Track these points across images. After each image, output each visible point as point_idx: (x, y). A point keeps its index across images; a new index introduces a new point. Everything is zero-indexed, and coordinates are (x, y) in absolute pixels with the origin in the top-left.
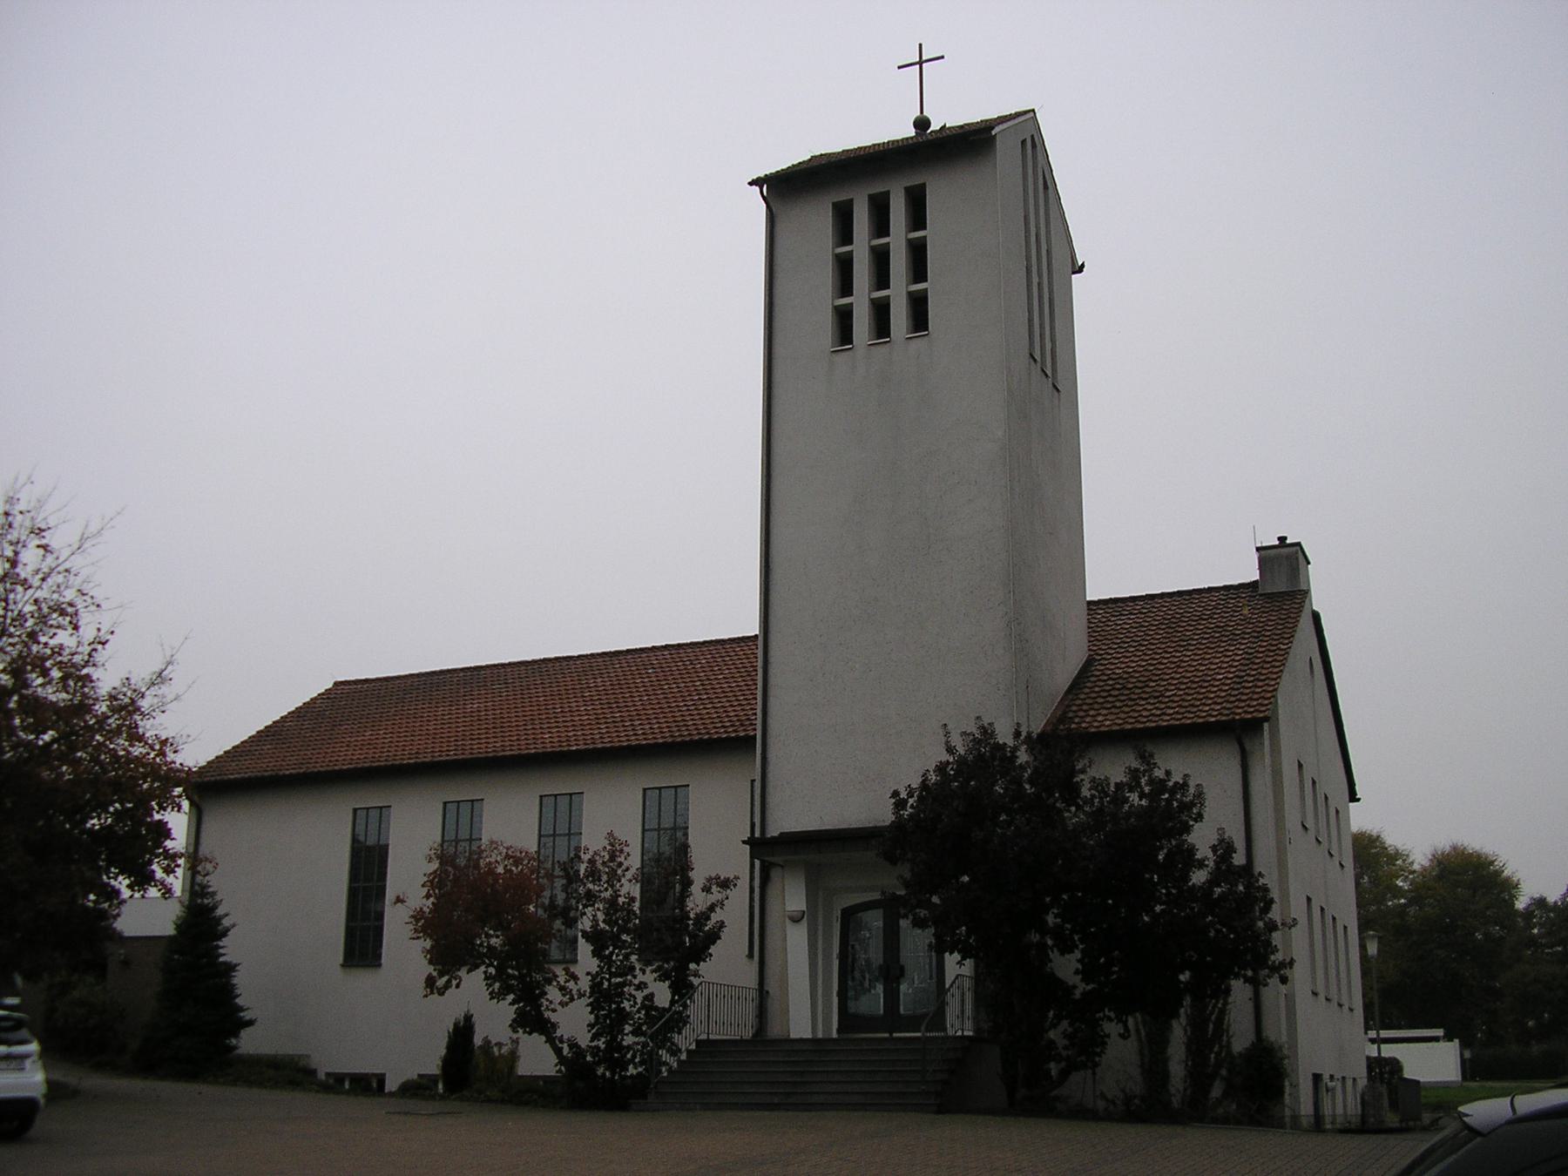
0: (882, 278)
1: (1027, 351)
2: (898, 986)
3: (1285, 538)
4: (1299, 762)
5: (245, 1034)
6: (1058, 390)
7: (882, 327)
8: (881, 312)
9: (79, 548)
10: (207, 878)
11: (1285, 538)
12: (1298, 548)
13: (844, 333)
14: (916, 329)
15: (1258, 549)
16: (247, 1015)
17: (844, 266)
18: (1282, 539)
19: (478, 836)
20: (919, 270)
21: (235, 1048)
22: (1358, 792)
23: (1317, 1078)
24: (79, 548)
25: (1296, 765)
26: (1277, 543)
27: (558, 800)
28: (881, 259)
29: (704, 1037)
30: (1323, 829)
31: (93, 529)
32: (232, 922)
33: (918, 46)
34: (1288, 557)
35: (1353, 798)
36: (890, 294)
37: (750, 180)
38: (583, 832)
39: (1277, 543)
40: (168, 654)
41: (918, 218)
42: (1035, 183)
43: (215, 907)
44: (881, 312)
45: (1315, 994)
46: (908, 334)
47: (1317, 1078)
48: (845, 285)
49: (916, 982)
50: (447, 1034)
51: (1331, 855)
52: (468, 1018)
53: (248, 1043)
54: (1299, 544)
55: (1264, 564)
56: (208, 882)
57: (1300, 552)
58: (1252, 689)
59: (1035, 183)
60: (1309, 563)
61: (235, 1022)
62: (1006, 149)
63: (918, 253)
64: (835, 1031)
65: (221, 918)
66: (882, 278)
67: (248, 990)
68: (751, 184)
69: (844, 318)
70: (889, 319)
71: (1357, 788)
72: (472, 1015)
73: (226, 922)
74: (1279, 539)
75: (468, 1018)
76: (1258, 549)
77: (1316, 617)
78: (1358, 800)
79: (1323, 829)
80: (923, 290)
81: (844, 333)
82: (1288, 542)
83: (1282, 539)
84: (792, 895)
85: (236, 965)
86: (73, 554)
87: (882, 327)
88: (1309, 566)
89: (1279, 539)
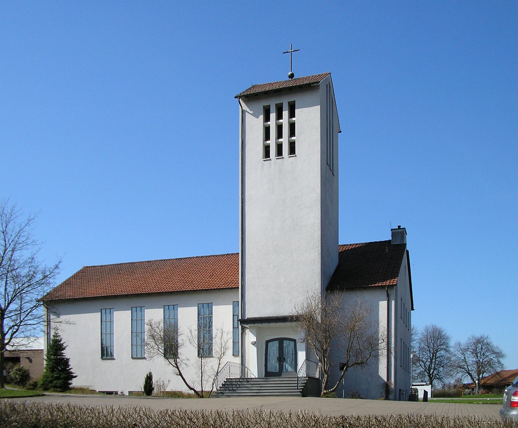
0: (280, 135)
1: (326, 163)
2: (283, 363)
3: (400, 226)
4: (401, 298)
5: (74, 379)
6: (334, 175)
7: (279, 152)
8: (279, 147)
9: (28, 224)
10: (57, 331)
11: (400, 226)
12: (404, 230)
13: (267, 154)
14: (290, 153)
15: (392, 230)
16: (74, 375)
17: (267, 130)
18: (399, 227)
19: (144, 319)
20: (292, 132)
21: (71, 384)
22: (414, 307)
23: (400, 390)
24: (28, 224)
25: (400, 299)
26: (398, 228)
27: (142, 309)
28: (280, 128)
29: (228, 378)
30: (405, 319)
31: (32, 217)
32: (67, 345)
33: (407, 233)
34: (401, 232)
35: (413, 309)
36: (283, 140)
37: (235, 96)
38: (145, 319)
39: (398, 228)
40: (60, 259)
41: (292, 114)
42: (330, 100)
43: (60, 341)
44: (279, 147)
45: (401, 366)
46: (288, 155)
47: (400, 390)
48: (267, 137)
49: (288, 362)
50: (145, 378)
51: (407, 326)
52: (150, 373)
53: (75, 383)
54: (405, 228)
55: (393, 235)
56: (58, 332)
57: (405, 231)
58: (364, 265)
59: (330, 100)
60: (407, 234)
61: (70, 376)
62: (322, 89)
63: (292, 126)
64: (264, 376)
65: (63, 344)
66: (280, 135)
67: (74, 366)
68: (235, 97)
69: (267, 149)
70: (282, 149)
71: (414, 306)
72: (151, 373)
73: (64, 345)
74: (398, 226)
75: (150, 373)
76: (392, 230)
77: (408, 252)
78: (414, 310)
79: (405, 319)
80: (294, 140)
81: (267, 154)
82: (401, 227)
83: (399, 227)
84: (250, 337)
85: (69, 359)
86: (26, 226)
87: (279, 152)
88: (407, 235)
89: (398, 226)
